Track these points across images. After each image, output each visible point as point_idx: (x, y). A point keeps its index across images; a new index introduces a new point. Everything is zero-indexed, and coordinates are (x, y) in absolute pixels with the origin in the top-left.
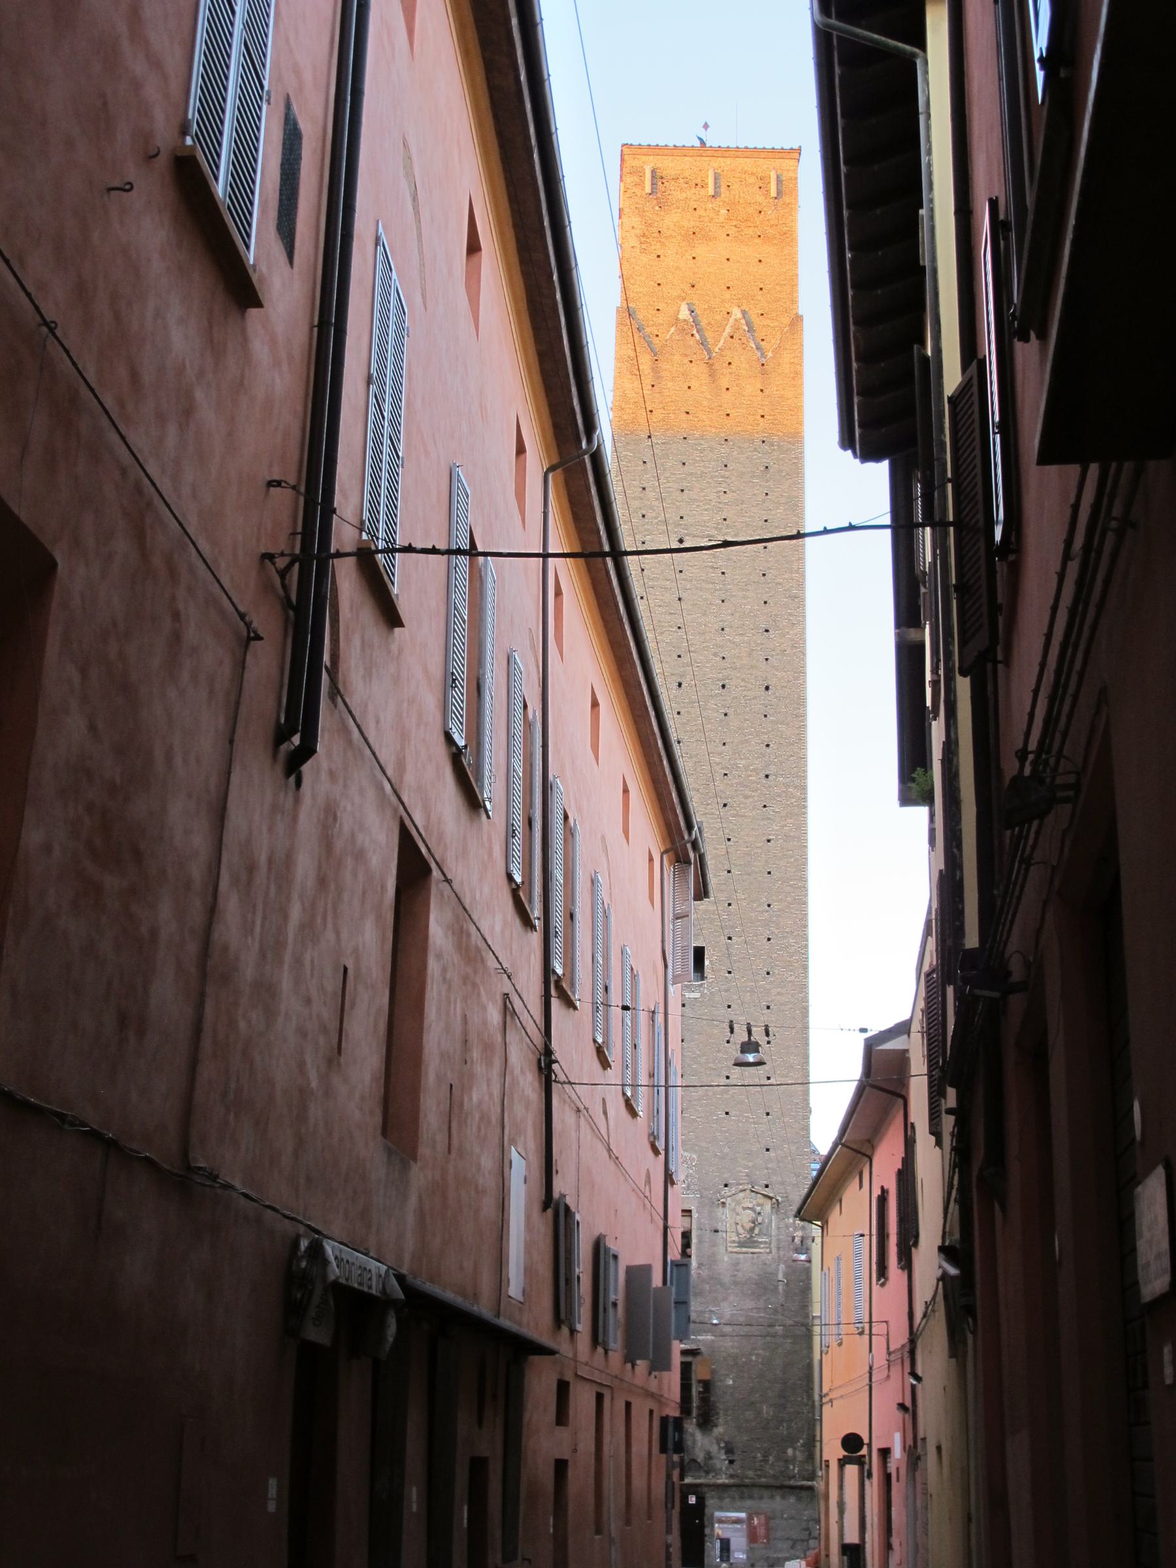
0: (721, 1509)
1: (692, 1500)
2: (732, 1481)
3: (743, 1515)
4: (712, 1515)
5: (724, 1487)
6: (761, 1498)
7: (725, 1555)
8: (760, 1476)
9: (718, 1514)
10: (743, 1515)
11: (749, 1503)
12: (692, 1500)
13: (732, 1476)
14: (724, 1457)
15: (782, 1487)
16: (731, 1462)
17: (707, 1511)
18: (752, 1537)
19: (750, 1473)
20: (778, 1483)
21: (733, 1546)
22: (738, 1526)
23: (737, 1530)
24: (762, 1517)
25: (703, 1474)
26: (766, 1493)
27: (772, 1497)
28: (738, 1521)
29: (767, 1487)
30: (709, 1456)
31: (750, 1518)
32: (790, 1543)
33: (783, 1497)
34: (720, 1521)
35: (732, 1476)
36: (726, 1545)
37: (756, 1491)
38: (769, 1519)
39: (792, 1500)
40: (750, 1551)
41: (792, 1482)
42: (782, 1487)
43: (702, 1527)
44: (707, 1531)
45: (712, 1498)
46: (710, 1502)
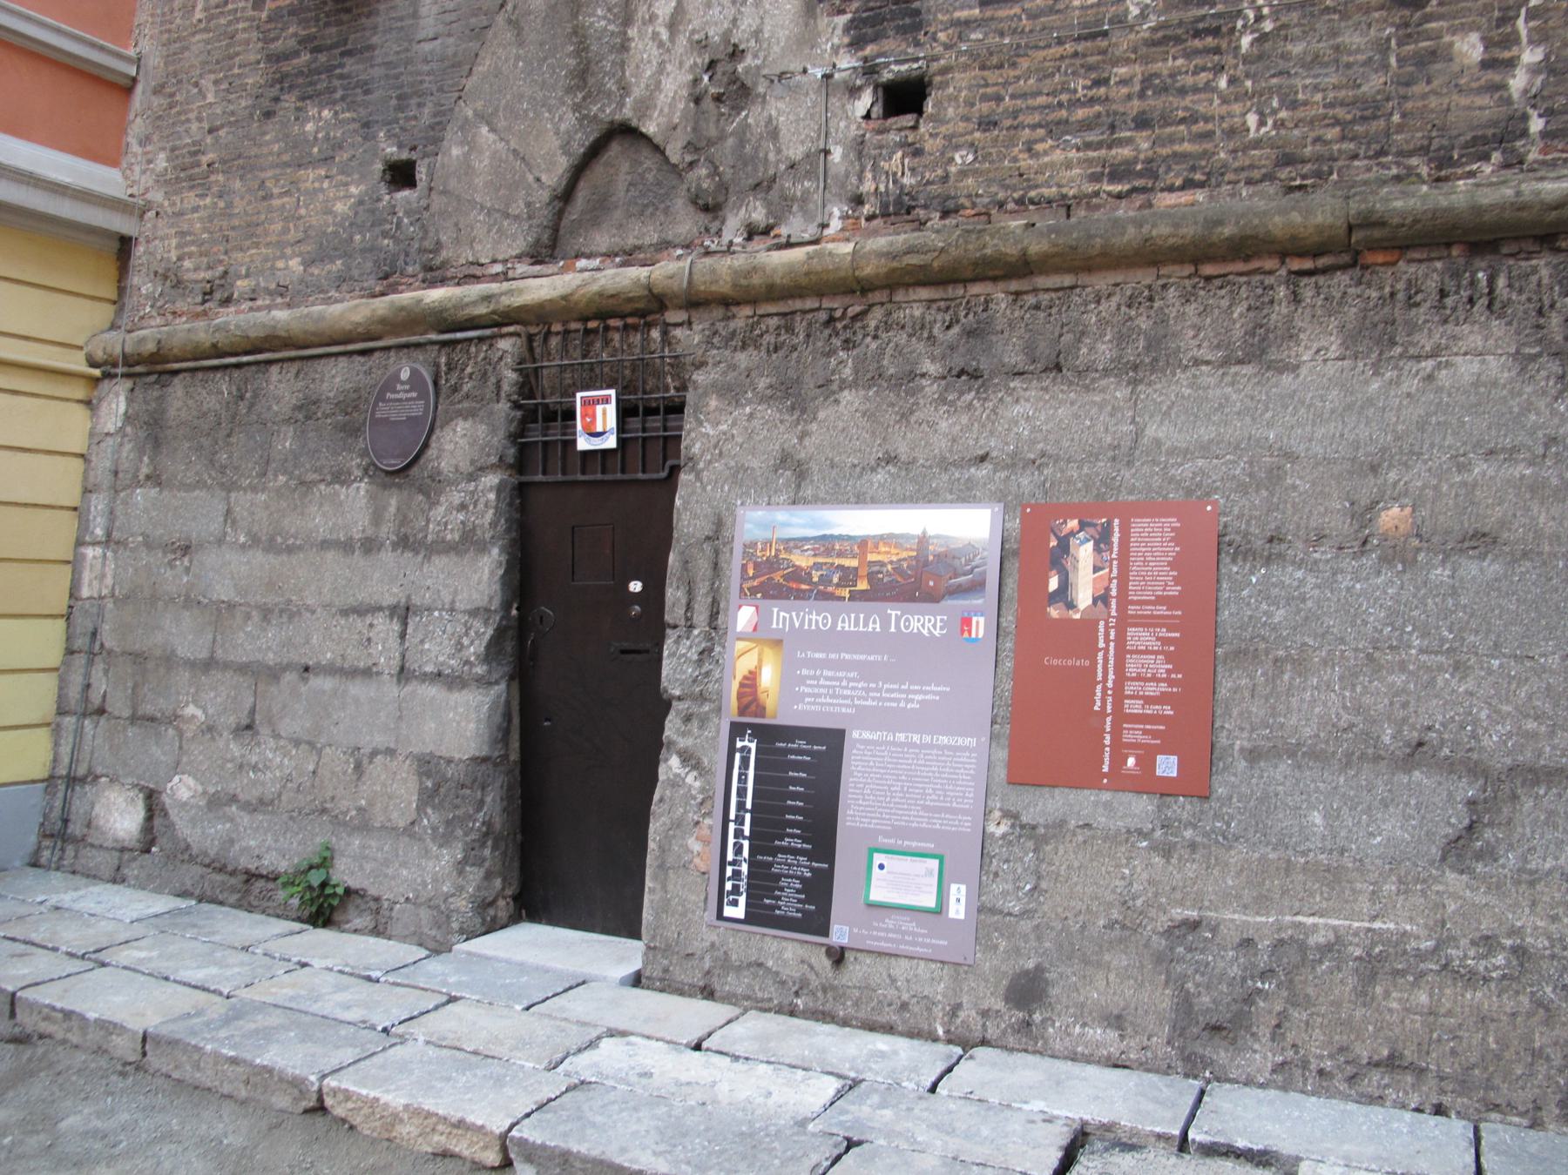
0: (796, 477)
1: (599, 424)
2: (884, 243)
3: (969, 526)
4: (718, 534)
5: (836, 304)
6: (1148, 361)
7: (794, 868)
8: (1141, 179)
9: (764, 523)
10: (969, 526)
11: (1028, 413)
12: (599, 424)
13: (899, 209)
14: (847, 62)
15: (1356, 247)
16: (904, 98)
17: (691, 508)
18: (1048, 731)
19: (1063, 165)
20: (1322, 211)
21: (859, 806)
22: (925, 622)
23: (909, 657)
24: (1154, 540)
25: (686, 223)
26: (1199, 318)
27: (1259, 350)
28: (920, 579)
29: (1210, 257)
30: (727, 81)
31: (1032, 553)
32: (1443, 800)
33: (1377, 339)
34: (778, 581)
35: (899, 209)
36: (798, 800)
37: (1099, 314)
38: (1216, 550)
39: (1478, 357)
40: (1008, 851)
41: (1482, 188)
42: (1356, 247)
43: (649, 629)
44: (677, 665)
45: (732, 393)
46: (707, 432)
